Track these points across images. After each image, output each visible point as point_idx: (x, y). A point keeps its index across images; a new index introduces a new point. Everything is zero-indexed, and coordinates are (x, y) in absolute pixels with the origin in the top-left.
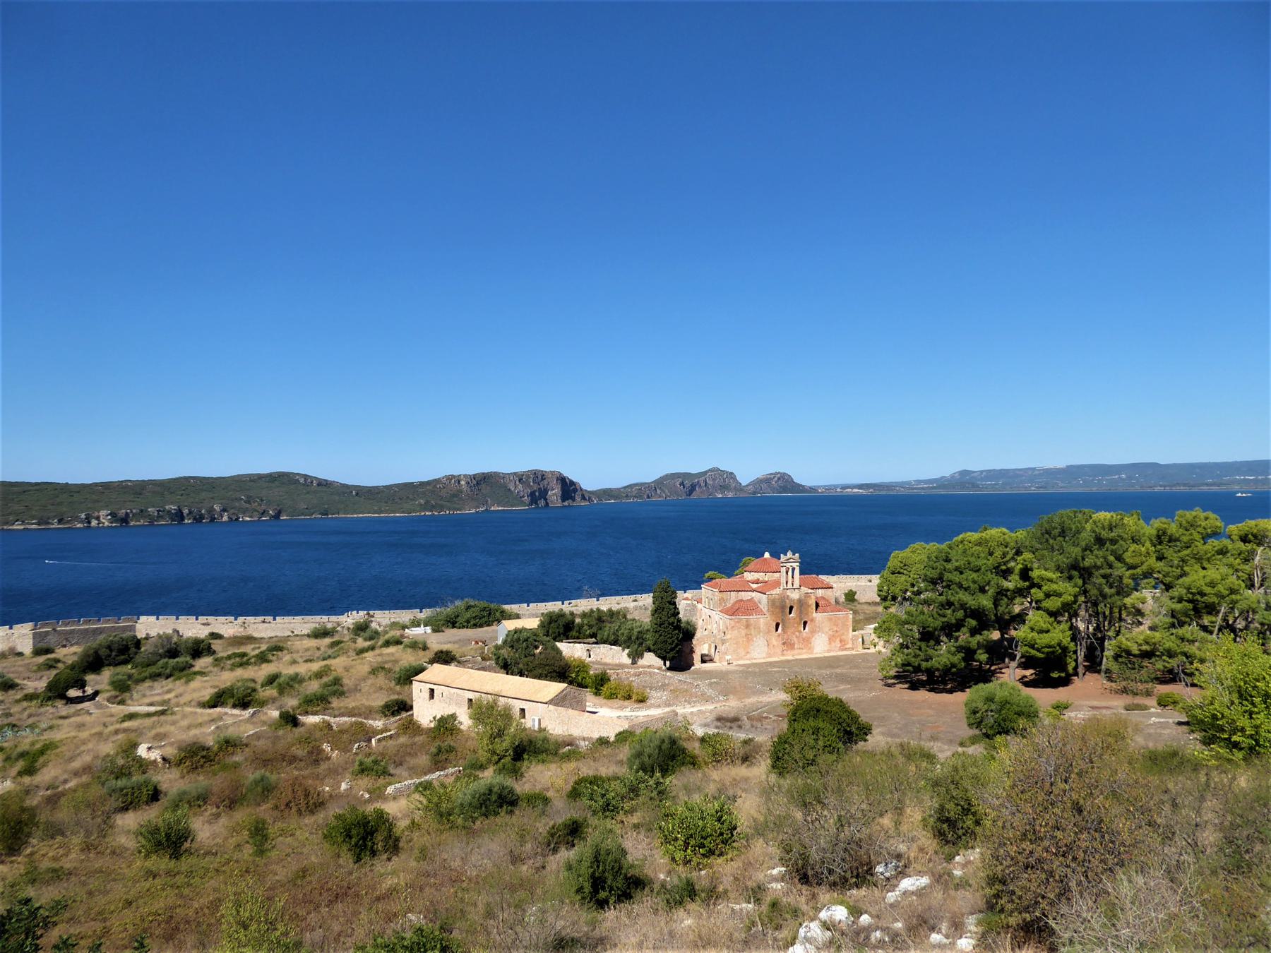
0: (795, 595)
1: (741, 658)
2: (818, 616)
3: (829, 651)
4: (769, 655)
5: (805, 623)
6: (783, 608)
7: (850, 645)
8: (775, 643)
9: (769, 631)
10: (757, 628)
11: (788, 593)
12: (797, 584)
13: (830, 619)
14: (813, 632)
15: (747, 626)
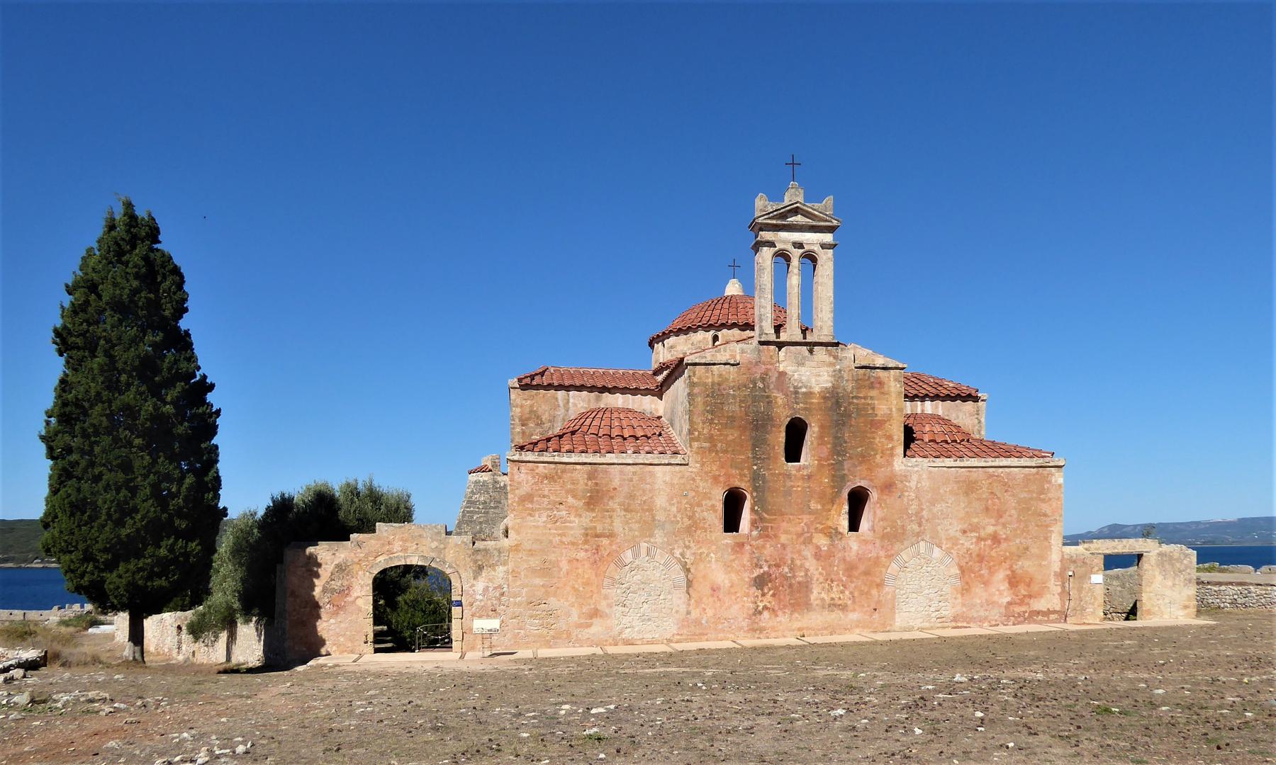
0: (812, 375)
1: (568, 638)
2: (917, 471)
4: (693, 627)
5: (858, 500)
6: (758, 425)
7: (1050, 601)
8: (721, 577)
9: (694, 527)
11: (785, 361)
12: (824, 327)
13: (969, 488)
14: (893, 536)
15: (595, 498)
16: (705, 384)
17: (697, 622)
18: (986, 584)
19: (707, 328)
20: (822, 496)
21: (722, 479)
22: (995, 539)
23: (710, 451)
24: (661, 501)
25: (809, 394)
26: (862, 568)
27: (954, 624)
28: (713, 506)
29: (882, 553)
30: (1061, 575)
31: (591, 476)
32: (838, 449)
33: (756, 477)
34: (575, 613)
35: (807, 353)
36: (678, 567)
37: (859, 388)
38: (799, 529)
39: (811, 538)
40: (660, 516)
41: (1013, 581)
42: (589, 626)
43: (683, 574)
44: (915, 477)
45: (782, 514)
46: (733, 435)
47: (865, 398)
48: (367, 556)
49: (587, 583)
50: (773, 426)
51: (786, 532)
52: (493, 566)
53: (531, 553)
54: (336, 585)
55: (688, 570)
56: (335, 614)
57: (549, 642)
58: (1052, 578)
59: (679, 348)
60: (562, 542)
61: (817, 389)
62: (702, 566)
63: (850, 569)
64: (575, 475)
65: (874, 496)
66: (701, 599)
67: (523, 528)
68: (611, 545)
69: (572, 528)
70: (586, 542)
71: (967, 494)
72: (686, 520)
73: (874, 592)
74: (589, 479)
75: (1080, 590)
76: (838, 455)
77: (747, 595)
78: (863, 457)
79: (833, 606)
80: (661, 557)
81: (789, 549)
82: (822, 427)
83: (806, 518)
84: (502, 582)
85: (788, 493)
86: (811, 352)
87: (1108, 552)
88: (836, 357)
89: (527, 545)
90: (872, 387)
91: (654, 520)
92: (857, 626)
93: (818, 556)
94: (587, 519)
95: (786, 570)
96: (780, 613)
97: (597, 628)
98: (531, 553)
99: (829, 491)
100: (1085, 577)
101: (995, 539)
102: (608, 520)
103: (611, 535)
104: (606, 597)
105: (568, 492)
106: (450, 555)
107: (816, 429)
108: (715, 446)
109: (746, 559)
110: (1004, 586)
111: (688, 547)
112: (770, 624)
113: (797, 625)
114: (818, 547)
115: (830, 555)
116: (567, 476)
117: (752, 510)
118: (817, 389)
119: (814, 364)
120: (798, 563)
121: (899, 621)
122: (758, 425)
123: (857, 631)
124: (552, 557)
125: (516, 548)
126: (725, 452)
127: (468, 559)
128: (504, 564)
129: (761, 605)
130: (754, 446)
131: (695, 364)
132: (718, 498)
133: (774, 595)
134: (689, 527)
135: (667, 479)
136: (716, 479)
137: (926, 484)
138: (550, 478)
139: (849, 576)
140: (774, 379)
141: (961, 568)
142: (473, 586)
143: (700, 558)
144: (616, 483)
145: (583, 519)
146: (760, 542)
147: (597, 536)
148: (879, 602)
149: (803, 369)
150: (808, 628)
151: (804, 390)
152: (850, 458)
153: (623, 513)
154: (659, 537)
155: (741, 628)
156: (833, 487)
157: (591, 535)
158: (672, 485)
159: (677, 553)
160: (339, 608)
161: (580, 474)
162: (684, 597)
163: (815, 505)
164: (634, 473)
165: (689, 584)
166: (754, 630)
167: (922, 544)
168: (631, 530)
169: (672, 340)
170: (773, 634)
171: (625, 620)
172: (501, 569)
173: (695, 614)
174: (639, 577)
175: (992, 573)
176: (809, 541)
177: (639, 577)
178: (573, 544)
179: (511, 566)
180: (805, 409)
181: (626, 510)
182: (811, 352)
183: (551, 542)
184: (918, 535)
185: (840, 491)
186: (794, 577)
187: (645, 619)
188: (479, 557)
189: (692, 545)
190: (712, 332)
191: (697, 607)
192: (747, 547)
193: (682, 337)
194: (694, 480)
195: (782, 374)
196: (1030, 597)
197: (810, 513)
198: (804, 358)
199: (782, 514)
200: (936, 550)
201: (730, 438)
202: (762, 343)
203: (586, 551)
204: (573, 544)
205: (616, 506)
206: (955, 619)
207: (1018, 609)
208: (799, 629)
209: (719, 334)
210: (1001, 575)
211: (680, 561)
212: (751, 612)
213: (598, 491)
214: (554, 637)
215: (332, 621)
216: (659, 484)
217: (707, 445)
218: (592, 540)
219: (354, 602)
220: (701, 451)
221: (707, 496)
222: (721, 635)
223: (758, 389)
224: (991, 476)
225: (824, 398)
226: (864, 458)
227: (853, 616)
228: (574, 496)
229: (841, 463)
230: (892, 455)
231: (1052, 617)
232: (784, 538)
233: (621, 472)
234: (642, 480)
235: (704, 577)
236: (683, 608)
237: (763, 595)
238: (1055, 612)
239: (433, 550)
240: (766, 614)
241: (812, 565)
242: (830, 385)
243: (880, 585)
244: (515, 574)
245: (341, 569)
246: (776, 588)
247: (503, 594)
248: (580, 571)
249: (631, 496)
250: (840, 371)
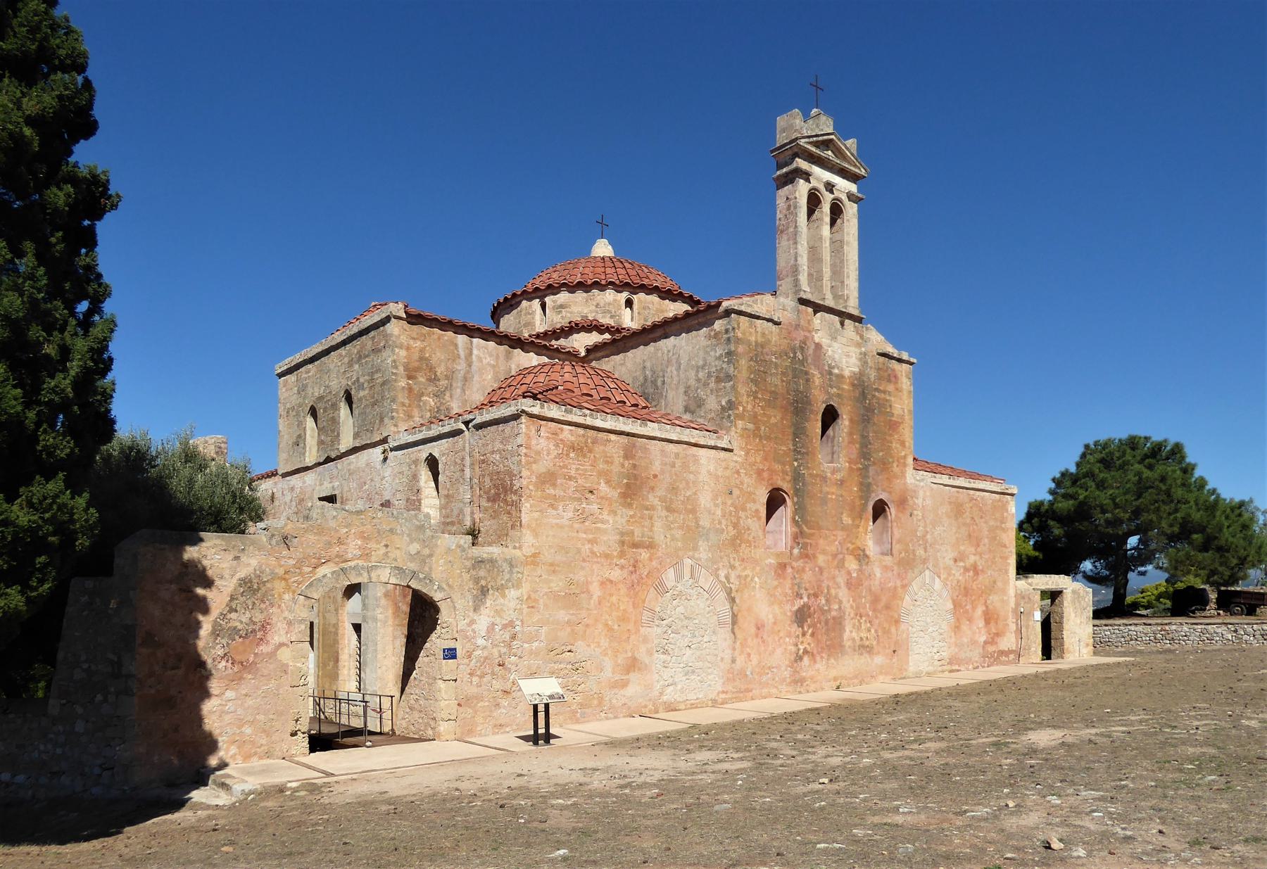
3: (954, 662)
6: (799, 406)
9: (737, 540)
10: (681, 506)
13: (958, 510)
14: (908, 564)
15: (633, 488)
16: (749, 344)
17: (742, 674)
18: (970, 620)
19: (619, 287)
20: (852, 509)
21: (765, 475)
22: (975, 568)
24: (705, 500)
25: (840, 377)
26: (884, 599)
27: (949, 667)
28: (757, 511)
29: (899, 583)
30: (1015, 611)
32: (865, 454)
33: (797, 477)
34: (608, 664)
35: (839, 325)
36: (723, 595)
37: (880, 378)
38: (833, 549)
39: (843, 560)
40: (705, 522)
41: (989, 617)
42: (624, 684)
44: (921, 493)
45: (820, 528)
46: (775, 417)
47: (884, 392)
48: (300, 564)
49: (623, 619)
50: (812, 412)
51: (824, 552)
52: (501, 589)
53: (553, 568)
54: (239, 620)
55: (733, 600)
56: (236, 679)
57: (575, 712)
58: (1010, 615)
59: (575, 309)
60: (593, 553)
61: (847, 373)
63: (876, 600)
64: (609, 446)
65: (892, 511)
66: (746, 640)
67: (542, 527)
68: (650, 559)
70: (622, 554)
71: (957, 519)
72: (731, 528)
73: (893, 630)
74: (626, 457)
75: (1027, 627)
76: (865, 458)
77: (789, 636)
78: (884, 464)
79: (864, 648)
80: (706, 580)
81: (825, 574)
82: (851, 420)
83: (840, 535)
84: (514, 616)
85: (824, 501)
86: (842, 324)
87: (1043, 588)
88: (862, 337)
89: (547, 556)
90: (889, 381)
91: (698, 526)
92: (881, 673)
93: (849, 585)
95: (823, 602)
96: (818, 658)
97: (634, 690)
98: (553, 568)
99: (858, 502)
100: (1031, 614)
101: (975, 570)
102: (647, 523)
103: (651, 546)
104: (646, 640)
105: (601, 474)
106: (439, 568)
107: (847, 423)
108: (758, 429)
109: (788, 583)
110: (981, 624)
111: (733, 567)
112: (811, 673)
113: (833, 673)
114: (849, 573)
115: (859, 583)
116: (598, 449)
117: (794, 519)
118: (847, 373)
119: (844, 340)
120: (833, 592)
121: (912, 668)
122: (799, 406)
123: (881, 678)
124: (580, 576)
125: (534, 560)
126: (769, 438)
127: (466, 576)
128: (518, 586)
129: (802, 647)
130: (796, 435)
131: (740, 313)
132: (763, 497)
133: (813, 635)
134: (734, 539)
135: (712, 468)
136: (759, 473)
137: (928, 502)
138: (579, 450)
139: (874, 610)
140: (811, 351)
141: (954, 603)
142: (472, 622)
143: (745, 582)
144: (656, 467)
145: (618, 518)
146: (800, 563)
148: (896, 643)
149: (835, 345)
150: (842, 677)
152: (874, 463)
153: (664, 513)
154: (703, 553)
155: (784, 680)
156: (861, 498)
157: (629, 544)
158: (717, 477)
159: (722, 574)
160: (246, 667)
162: (729, 636)
163: (847, 520)
164: (677, 455)
166: (795, 682)
167: (927, 572)
169: (563, 296)
170: (813, 687)
171: (666, 674)
172: (512, 593)
173: (740, 661)
174: (680, 609)
175: (974, 608)
176: (841, 565)
177: (680, 609)
178: (607, 556)
179: (525, 589)
180: (839, 395)
181: (669, 509)
182: (842, 324)
183: (579, 551)
184: (925, 561)
185: (865, 505)
186: (829, 610)
187: (689, 671)
188: (482, 573)
189: (737, 564)
190: (625, 295)
192: (789, 570)
193: (580, 295)
194: (738, 472)
195: (818, 346)
196: (997, 635)
197: (843, 529)
198: (837, 330)
199: (820, 528)
200: (937, 580)
201: (773, 420)
202: (803, 302)
203: (622, 567)
204: (607, 556)
205: (656, 502)
206: (950, 663)
207: (991, 649)
208: (835, 679)
209: (635, 298)
210: (980, 610)
211: (725, 587)
212: (793, 658)
214: (582, 705)
215: (230, 694)
217: (750, 426)
218: (630, 552)
219: (273, 654)
220: (745, 434)
221: (750, 496)
222: (765, 691)
223: (800, 359)
224: (972, 499)
225: (853, 385)
226: (885, 465)
227: (879, 660)
228: (608, 482)
229: (866, 468)
230: (905, 465)
231: (1012, 656)
232: (821, 559)
234: (685, 466)
235: (749, 609)
236: (727, 655)
237: (804, 634)
238: (1011, 652)
239: (412, 557)
240: (806, 659)
241: (843, 593)
242: (857, 370)
243: (897, 622)
244: (531, 602)
245: (251, 587)
246: (813, 625)
247: (514, 637)
248: (614, 599)
249: (674, 489)
250: (865, 354)
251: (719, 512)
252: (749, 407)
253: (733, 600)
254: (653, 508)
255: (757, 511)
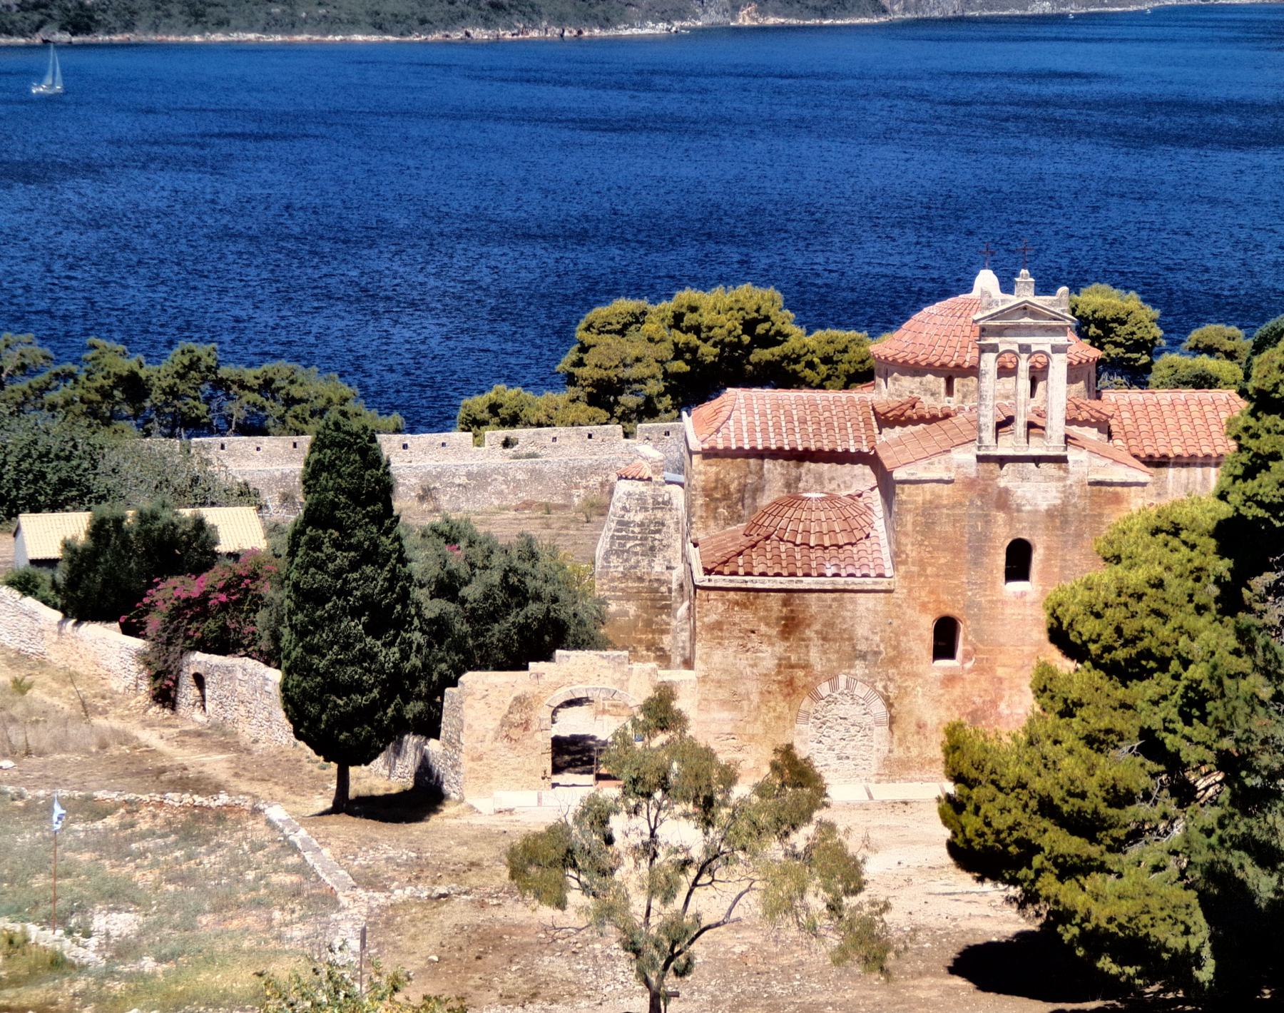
23: (920, 575)
28: (920, 635)
31: (785, 603)
43: (884, 709)
62: (906, 701)
66: (905, 736)
68: (806, 676)
69: (764, 658)
70: (779, 673)
89: (714, 675)
94: (780, 647)
102: (804, 650)
108: (925, 570)
111: (890, 679)
138: (743, 605)
144: (814, 609)
145: (776, 649)
147: (792, 667)
151: (1028, 508)
157: (785, 665)
158: (876, 612)
159: (880, 686)
161: (774, 601)
164: (834, 600)
165: (892, 721)
168: (829, 660)
181: (824, 639)
189: (897, 677)
191: (900, 745)
201: (942, 561)
205: (813, 635)
213: (793, 618)
216: (861, 609)
228: (767, 624)
233: (819, 599)
235: (910, 712)
248: (772, 704)
249: (830, 624)
251: (877, 638)
252: (914, 554)
253: (890, 705)
254: (810, 639)
255: (920, 635)
